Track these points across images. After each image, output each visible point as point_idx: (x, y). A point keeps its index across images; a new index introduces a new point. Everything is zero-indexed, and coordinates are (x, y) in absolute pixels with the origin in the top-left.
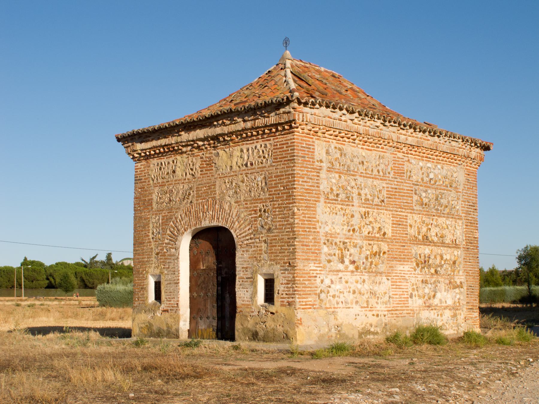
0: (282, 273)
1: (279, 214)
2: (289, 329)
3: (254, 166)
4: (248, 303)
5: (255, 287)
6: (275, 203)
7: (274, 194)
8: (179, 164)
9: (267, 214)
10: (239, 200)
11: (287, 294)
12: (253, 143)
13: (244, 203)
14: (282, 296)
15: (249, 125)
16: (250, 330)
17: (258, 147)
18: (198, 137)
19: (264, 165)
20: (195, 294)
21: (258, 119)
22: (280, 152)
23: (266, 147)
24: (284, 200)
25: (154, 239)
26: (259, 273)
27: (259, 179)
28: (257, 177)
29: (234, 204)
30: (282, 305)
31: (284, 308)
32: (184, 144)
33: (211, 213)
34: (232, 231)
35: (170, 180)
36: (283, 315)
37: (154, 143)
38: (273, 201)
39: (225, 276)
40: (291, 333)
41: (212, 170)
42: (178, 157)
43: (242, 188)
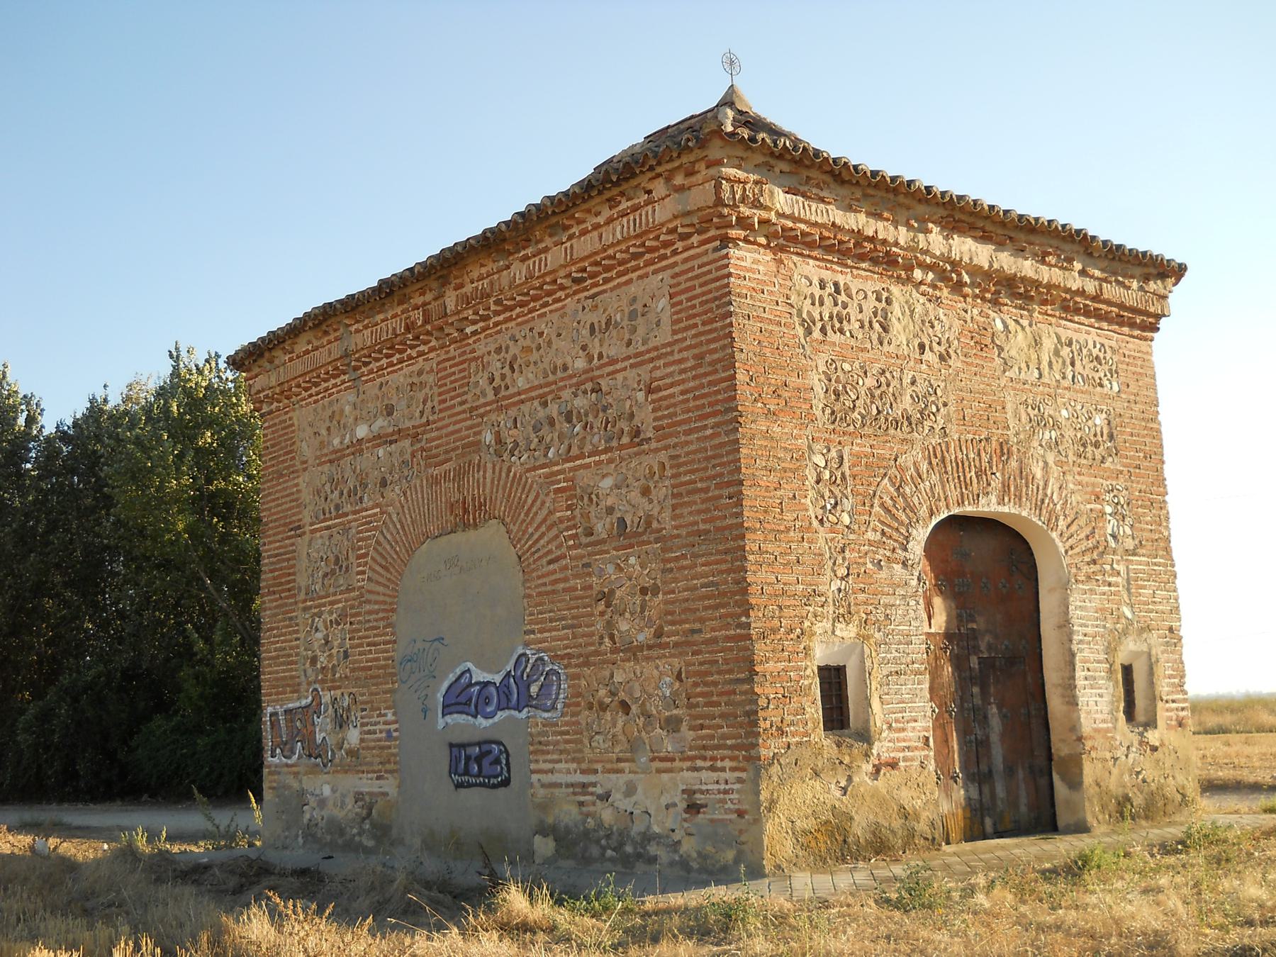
32: (928, 260)
35: (869, 346)
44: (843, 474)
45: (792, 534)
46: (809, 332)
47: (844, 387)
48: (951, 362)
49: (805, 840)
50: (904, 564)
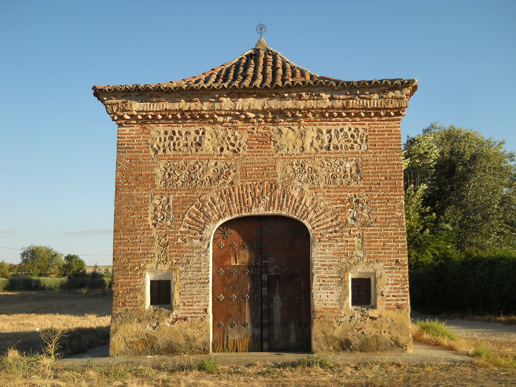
0: (388, 272)
1: (381, 207)
2: (399, 335)
3: (340, 150)
4: (334, 307)
5: (346, 287)
6: (374, 193)
7: (371, 184)
8: (207, 135)
9: (360, 205)
10: (316, 186)
11: (394, 296)
12: (339, 125)
13: (325, 190)
14: (387, 298)
15: (338, 104)
16: (336, 339)
17: (346, 129)
18: (252, 108)
19: (355, 150)
20: (222, 297)
21: (353, 99)
22: (378, 138)
24: (387, 192)
25: (158, 226)
26: (352, 271)
27: (348, 165)
28: (345, 162)
29: (308, 190)
30: (387, 309)
31: (391, 313)
32: (223, 113)
33: (268, 199)
34: (305, 222)
35: (190, 153)
36: (389, 320)
37: (168, 105)
38: (370, 191)
39: (273, 274)
41: (270, 148)
42: (208, 128)
43: (321, 174)
44: (169, 207)
45: (138, 231)
46: (156, 152)
47: (174, 172)
48: (240, 153)
50: (201, 240)
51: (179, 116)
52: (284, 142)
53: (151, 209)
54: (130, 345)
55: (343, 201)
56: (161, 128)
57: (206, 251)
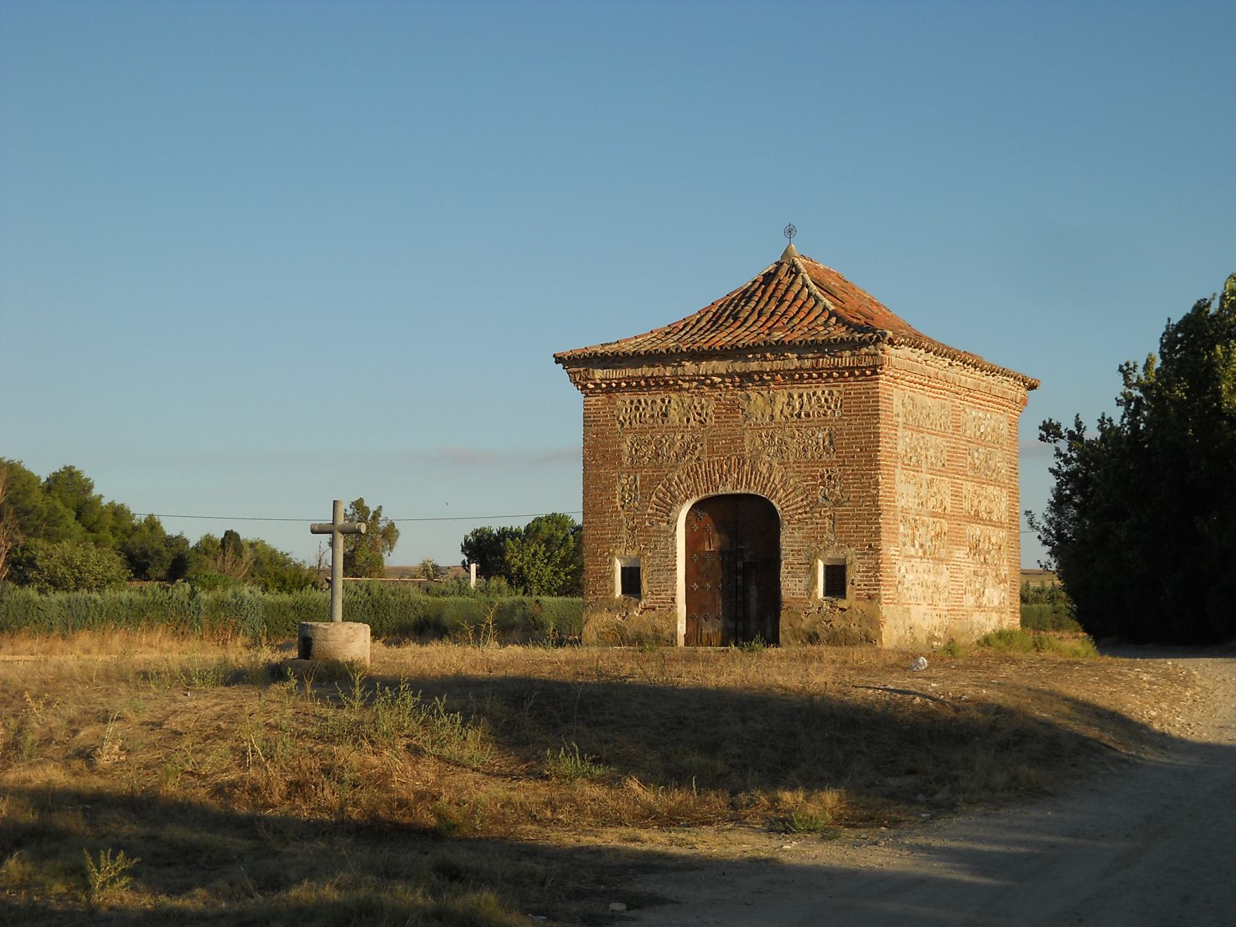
5: (815, 576)
8: (673, 404)
20: (695, 586)
23: (831, 393)
27: (820, 436)
30: (858, 599)
31: (861, 603)
34: (773, 501)
37: (630, 372)
40: (872, 633)
42: (673, 396)
46: (622, 425)
49: (601, 636)
51: (643, 383)
52: (752, 410)
53: (619, 489)
54: (601, 636)
55: (814, 478)
56: (627, 397)
57: (673, 535)
